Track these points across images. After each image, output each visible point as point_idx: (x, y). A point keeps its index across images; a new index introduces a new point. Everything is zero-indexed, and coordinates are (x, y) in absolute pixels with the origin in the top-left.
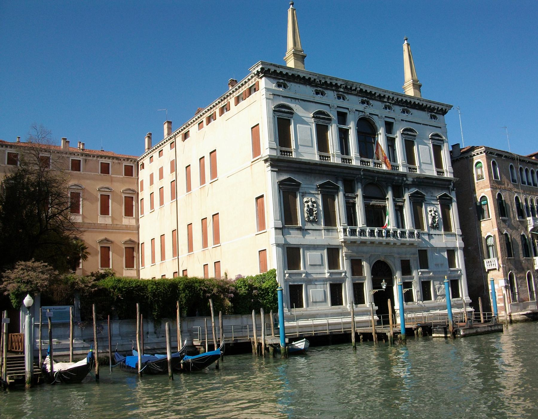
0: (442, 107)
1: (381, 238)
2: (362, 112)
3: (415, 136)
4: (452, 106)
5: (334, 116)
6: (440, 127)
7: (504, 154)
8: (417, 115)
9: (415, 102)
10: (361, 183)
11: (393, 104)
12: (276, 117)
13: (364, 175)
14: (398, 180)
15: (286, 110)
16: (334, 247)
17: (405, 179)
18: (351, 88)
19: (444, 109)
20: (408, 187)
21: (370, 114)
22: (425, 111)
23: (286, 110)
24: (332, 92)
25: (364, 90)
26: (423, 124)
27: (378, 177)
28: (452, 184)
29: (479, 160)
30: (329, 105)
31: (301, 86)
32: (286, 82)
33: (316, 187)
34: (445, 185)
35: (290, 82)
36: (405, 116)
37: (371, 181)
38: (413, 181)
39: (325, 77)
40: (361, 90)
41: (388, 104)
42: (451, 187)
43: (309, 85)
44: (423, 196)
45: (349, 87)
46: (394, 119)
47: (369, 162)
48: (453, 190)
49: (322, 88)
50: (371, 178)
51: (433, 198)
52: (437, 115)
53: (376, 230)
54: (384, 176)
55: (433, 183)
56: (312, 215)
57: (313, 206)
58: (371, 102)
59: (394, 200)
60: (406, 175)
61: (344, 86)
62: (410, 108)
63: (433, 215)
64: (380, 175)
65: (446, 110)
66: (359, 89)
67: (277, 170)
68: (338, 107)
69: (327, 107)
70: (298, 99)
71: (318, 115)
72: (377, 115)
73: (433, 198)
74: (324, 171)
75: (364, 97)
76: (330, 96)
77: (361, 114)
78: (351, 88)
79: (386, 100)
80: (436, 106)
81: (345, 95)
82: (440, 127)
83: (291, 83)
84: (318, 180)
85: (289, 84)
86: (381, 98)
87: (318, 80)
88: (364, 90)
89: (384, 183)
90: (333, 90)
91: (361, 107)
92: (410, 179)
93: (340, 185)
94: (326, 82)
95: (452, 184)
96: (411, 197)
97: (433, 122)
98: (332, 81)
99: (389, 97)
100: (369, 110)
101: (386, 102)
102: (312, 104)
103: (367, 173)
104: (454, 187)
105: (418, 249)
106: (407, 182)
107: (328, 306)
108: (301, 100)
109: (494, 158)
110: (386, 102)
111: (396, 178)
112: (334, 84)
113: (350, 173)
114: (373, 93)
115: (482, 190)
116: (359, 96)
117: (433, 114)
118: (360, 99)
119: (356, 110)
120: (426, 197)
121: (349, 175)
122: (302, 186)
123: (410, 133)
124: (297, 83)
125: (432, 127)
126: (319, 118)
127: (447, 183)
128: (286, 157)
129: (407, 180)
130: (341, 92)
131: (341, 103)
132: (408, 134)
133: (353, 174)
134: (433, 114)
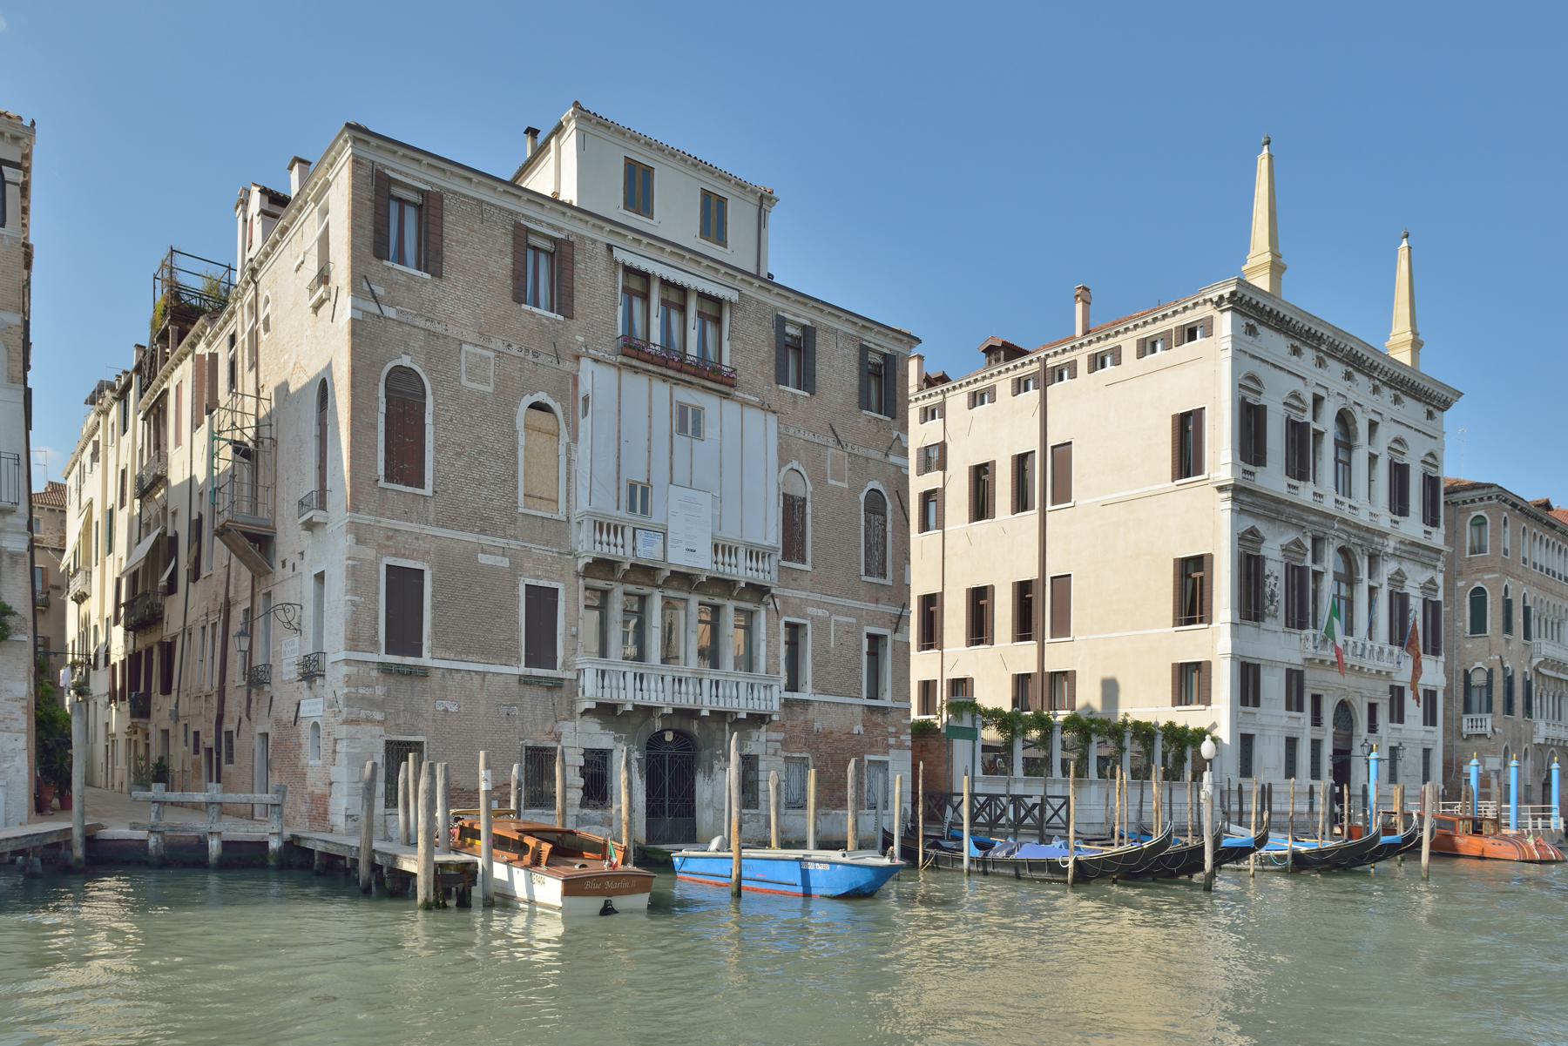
29: (1481, 513)
84: (1282, 534)
92: (1391, 545)
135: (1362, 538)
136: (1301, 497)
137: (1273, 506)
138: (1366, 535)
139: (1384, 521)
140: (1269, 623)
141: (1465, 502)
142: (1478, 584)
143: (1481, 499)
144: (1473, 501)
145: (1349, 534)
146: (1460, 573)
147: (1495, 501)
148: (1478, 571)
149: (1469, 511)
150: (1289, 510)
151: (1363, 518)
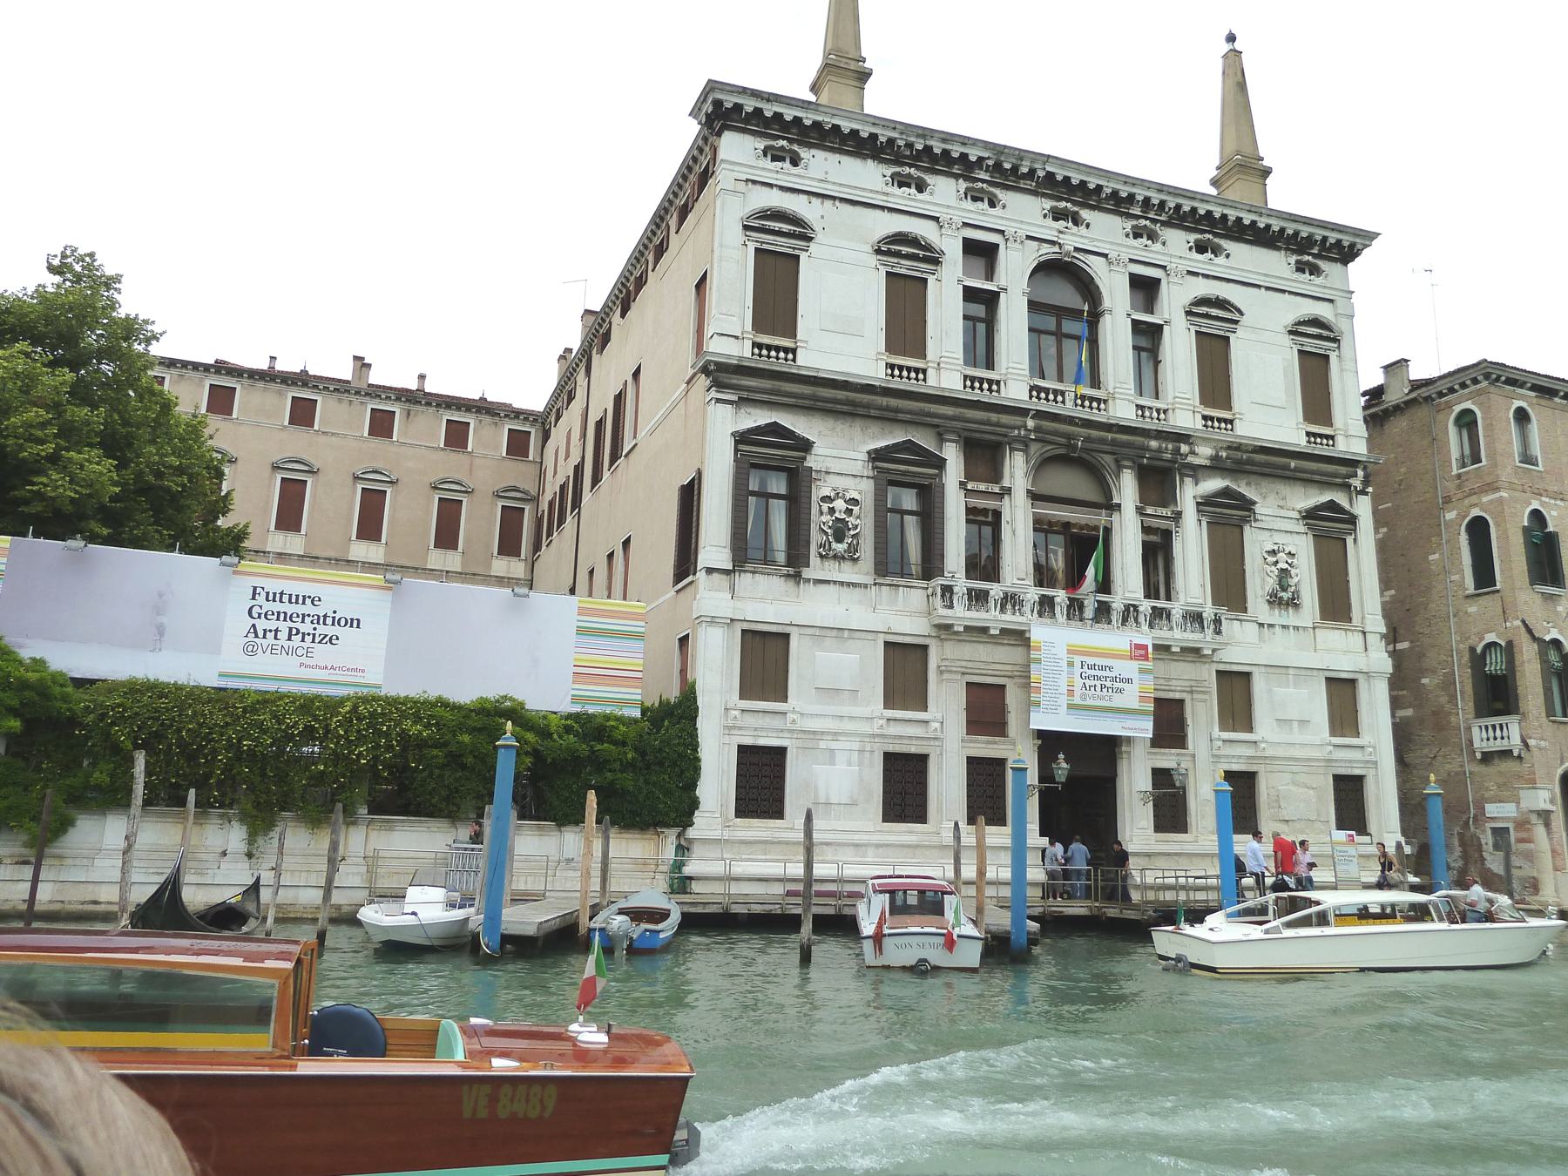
0: (1340, 236)
2: (1053, 243)
3: (1236, 322)
4: (1372, 236)
5: (952, 248)
6: (1331, 301)
8: (1243, 258)
9: (1239, 219)
10: (1026, 451)
11: (1164, 224)
12: (752, 247)
13: (1037, 429)
14: (1159, 450)
15: (786, 227)
16: (908, 640)
17: (1184, 448)
18: (1015, 169)
19: (1346, 244)
20: (1196, 472)
21: (1077, 249)
22: (1278, 249)
23: (786, 227)
24: (953, 181)
25: (1059, 178)
26: (1268, 288)
27: (1087, 439)
28: (1360, 473)
29: (1468, 405)
30: (936, 219)
31: (848, 161)
32: (795, 147)
33: (865, 457)
34: (1335, 475)
35: (810, 146)
36: (1201, 262)
37: (1062, 451)
38: (1215, 458)
39: (925, 133)
40: (1050, 175)
41: (1143, 222)
42: (1356, 483)
45: (1007, 166)
46: (1164, 267)
47: (1063, 393)
48: (1363, 492)
49: (918, 168)
50: (1063, 440)
51: (1283, 513)
52: (1320, 263)
54: (1110, 436)
55: (1286, 467)
56: (839, 540)
57: (849, 512)
58: (1085, 214)
59: (1140, 511)
60: (1189, 436)
61: (990, 163)
63: (1282, 565)
64: (1095, 433)
65: (1352, 245)
66: (1041, 173)
67: (735, 398)
68: (965, 224)
69: (932, 224)
70: (834, 198)
71: (895, 245)
72: (1105, 256)
73: (1283, 513)
74: (897, 410)
75: (1060, 199)
76: (944, 192)
77: (1046, 249)
78: (1015, 169)
79: (1137, 211)
80: (1319, 234)
81: (997, 191)
82: (1331, 301)
83: (813, 152)
84: (873, 438)
85: (804, 153)
87: (901, 143)
88: (1059, 178)
89: (1108, 459)
90: (956, 177)
91: (1050, 229)
92: (1204, 453)
93: (952, 455)
94: (928, 149)
95: (1360, 473)
96: (1205, 504)
97: (1304, 282)
98: (948, 147)
99: (1147, 200)
100: (1072, 238)
102: (878, 212)
103: (1046, 424)
104: (1366, 482)
105: (1215, 667)
106: (1190, 459)
107: (868, 821)
108: (842, 200)
109: (1522, 397)
110: (1137, 217)
111: (1154, 444)
112: (956, 155)
113: (988, 423)
114: (1091, 186)
115: (1474, 499)
116: (1044, 195)
117: (1306, 258)
118: (1048, 204)
119: (1029, 237)
120: (1258, 509)
122: (816, 450)
123: (1214, 312)
124: (832, 150)
125: (1299, 299)
126: (898, 254)
127: (1343, 470)
128: (778, 363)
129: (1193, 453)
130: (983, 181)
131: (978, 212)
132: (1207, 316)
133: (998, 425)
134: (1306, 258)
136: (930, 382)
139: (1186, 418)
140: (816, 568)
141: (1441, 395)
142: (1476, 512)
143: (1463, 386)
144: (1452, 390)
145: (1069, 437)
146: (1447, 500)
147: (1485, 384)
148: (1472, 493)
149: (1449, 406)
151: (1123, 411)
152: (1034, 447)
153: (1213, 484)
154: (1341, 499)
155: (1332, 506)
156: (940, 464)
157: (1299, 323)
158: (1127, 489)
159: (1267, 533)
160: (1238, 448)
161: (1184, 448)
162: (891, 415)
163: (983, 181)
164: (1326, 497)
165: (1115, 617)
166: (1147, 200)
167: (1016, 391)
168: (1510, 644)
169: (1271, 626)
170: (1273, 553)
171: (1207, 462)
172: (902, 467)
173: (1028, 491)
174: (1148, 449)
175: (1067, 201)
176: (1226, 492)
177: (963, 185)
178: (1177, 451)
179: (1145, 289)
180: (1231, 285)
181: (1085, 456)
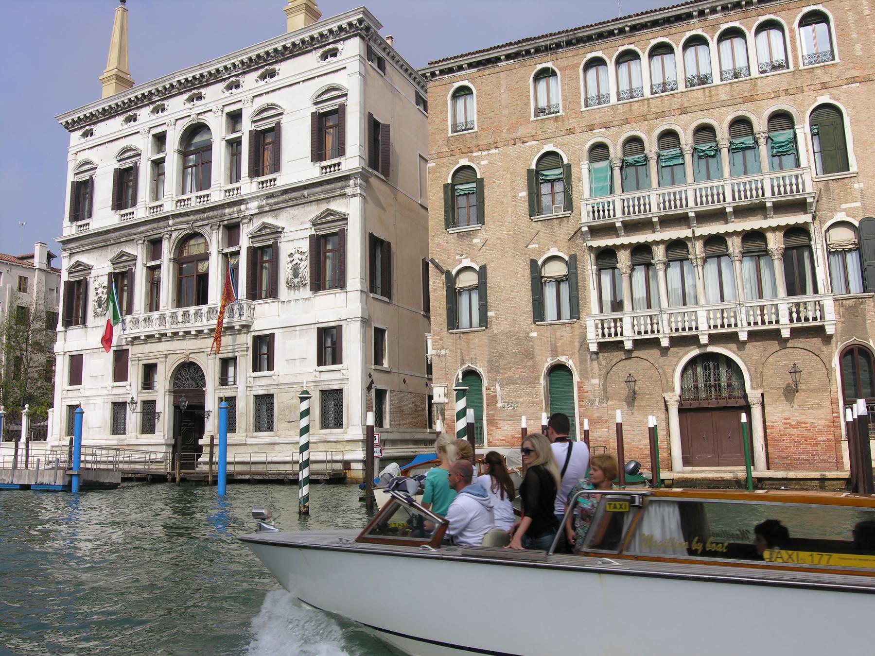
1: (175, 326)
2: (190, 116)
7: (502, 53)
14: (230, 214)
21: (199, 114)
43: (118, 115)
44: (277, 232)
53: (192, 309)
60: (243, 200)
62: (277, 62)
75: (190, 90)
77: (187, 120)
86: (214, 78)
89: (208, 228)
90: (148, 105)
92: (253, 206)
101: (229, 78)
106: (248, 213)
110: (229, 78)
111: (227, 211)
113: (154, 229)
116: (185, 92)
121: (154, 232)
130: (158, 101)
135: (208, 218)
137: (100, 238)
138: (211, 214)
145: (187, 222)
150: (114, 235)
152: (174, 235)
153: (257, 223)
154: (334, 206)
155: (330, 213)
156: (135, 258)
157: (323, 93)
158: (215, 241)
159: (291, 243)
160: (272, 195)
161: (243, 207)
162: (118, 241)
163: (158, 101)
164: (323, 207)
165: (192, 318)
166: (226, 68)
167: (169, 207)
168: (483, 269)
169: (289, 301)
170: (291, 255)
171: (256, 211)
172: (122, 265)
173: (170, 259)
174: (224, 215)
175: (194, 89)
176: (265, 226)
177: (152, 107)
178: (240, 211)
179: (235, 118)
180: (282, 90)
181: (197, 230)
